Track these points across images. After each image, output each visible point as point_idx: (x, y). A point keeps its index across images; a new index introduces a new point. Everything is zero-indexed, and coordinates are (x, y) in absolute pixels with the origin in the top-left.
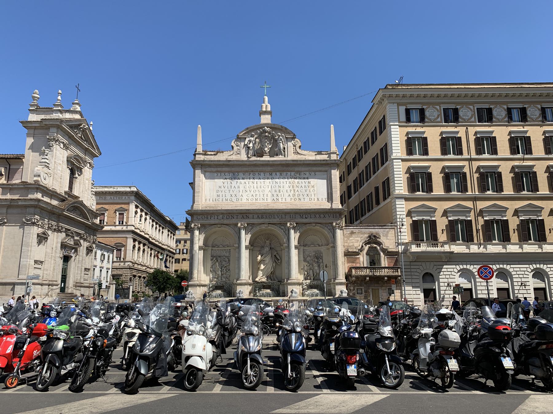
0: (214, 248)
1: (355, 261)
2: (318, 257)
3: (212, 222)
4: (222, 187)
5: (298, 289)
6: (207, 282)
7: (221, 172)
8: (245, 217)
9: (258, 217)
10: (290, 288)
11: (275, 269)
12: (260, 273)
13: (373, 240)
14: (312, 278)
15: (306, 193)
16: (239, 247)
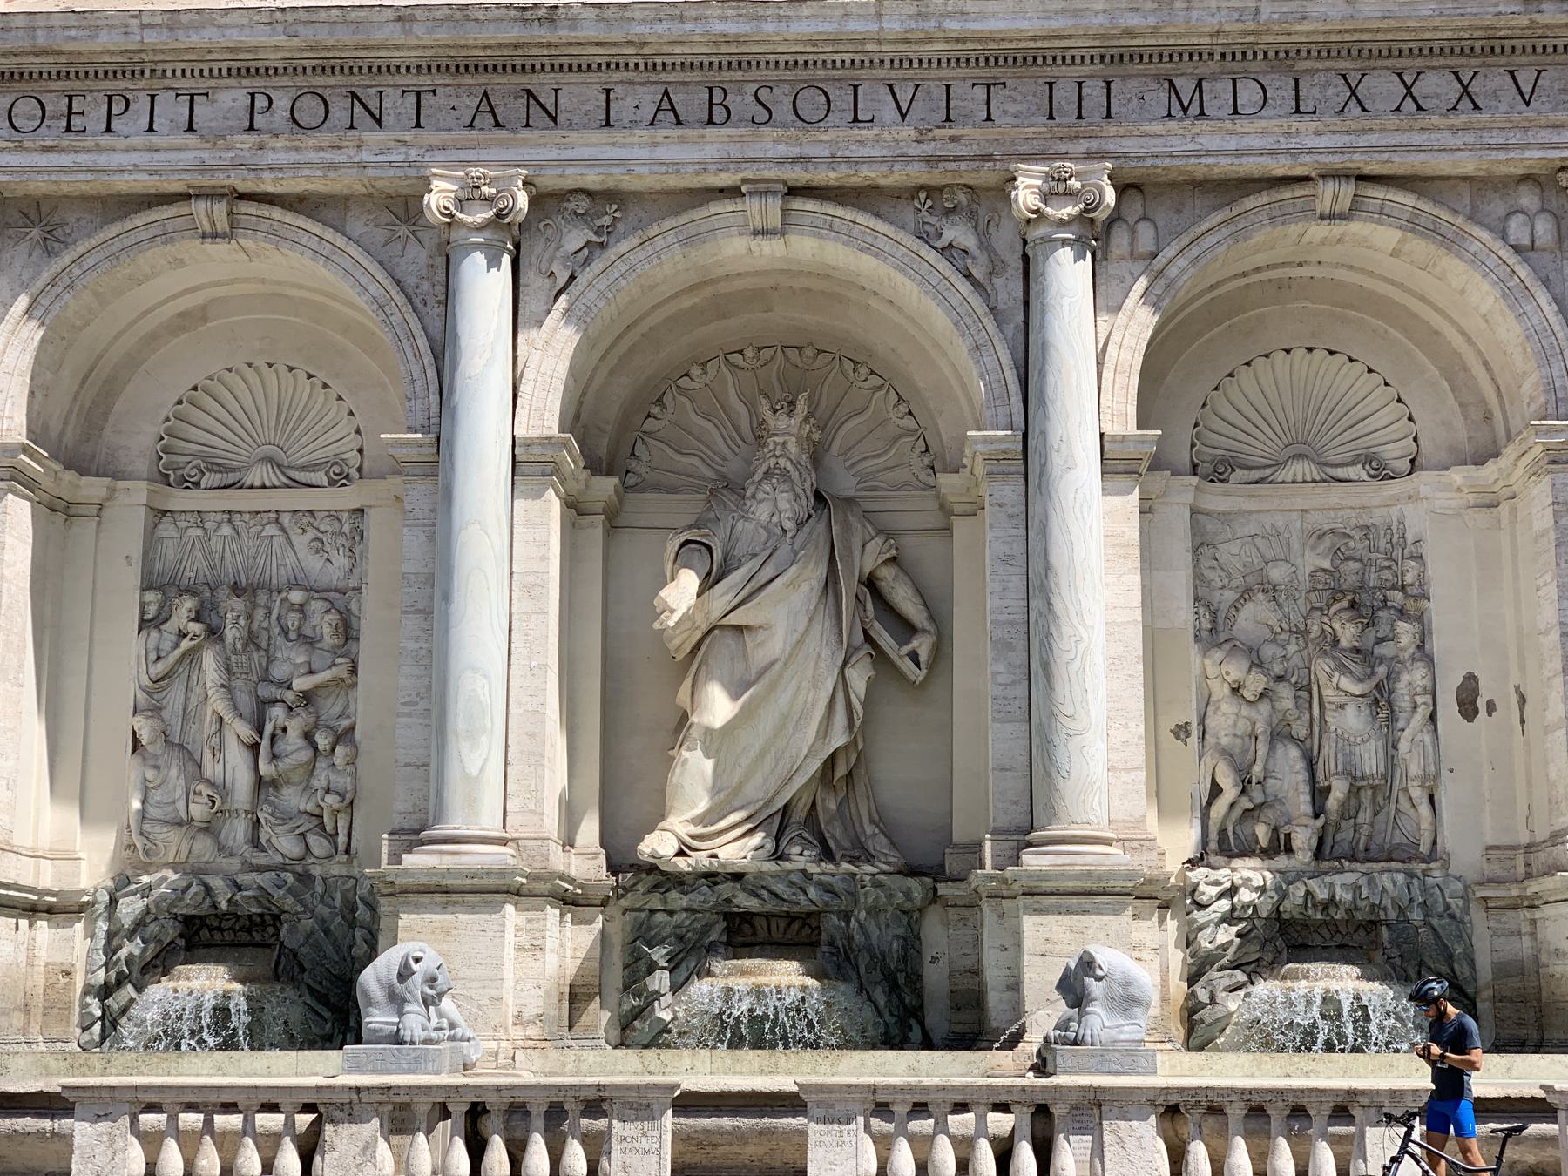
0: (182, 500)
2: (1371, 601)
3: (128, 158)
5: (1142, 957)
6: (89, 863)
8: (510, 108)
9: (668, 112)
10: (1046, 943)
11: (862, 730)
12: (695, 770)
14: (1303, 838)
16: (434, 464)
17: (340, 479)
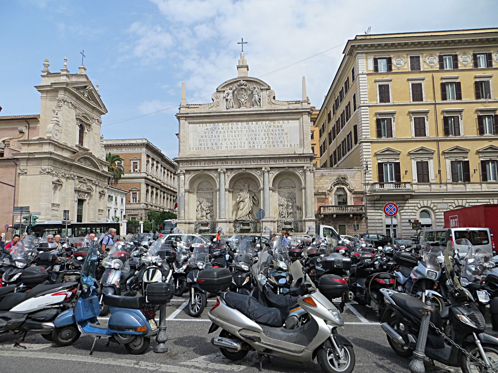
1: (325, 201)
7: (202, 123)
13: (341, 181)
15: (279, 140)
17: (211, 189)
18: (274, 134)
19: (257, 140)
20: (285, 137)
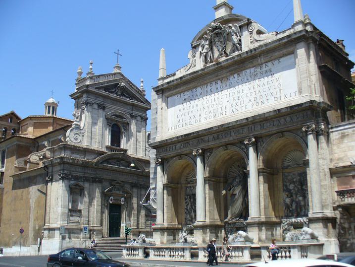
4: (182, 110)
7: (180, 93)
18: (261, 85)
19: (241, 99)
20: (276, 86)
